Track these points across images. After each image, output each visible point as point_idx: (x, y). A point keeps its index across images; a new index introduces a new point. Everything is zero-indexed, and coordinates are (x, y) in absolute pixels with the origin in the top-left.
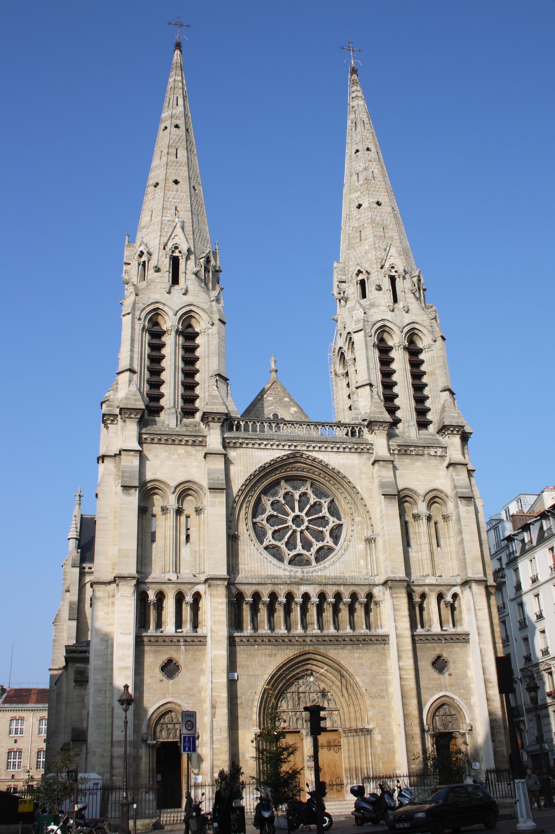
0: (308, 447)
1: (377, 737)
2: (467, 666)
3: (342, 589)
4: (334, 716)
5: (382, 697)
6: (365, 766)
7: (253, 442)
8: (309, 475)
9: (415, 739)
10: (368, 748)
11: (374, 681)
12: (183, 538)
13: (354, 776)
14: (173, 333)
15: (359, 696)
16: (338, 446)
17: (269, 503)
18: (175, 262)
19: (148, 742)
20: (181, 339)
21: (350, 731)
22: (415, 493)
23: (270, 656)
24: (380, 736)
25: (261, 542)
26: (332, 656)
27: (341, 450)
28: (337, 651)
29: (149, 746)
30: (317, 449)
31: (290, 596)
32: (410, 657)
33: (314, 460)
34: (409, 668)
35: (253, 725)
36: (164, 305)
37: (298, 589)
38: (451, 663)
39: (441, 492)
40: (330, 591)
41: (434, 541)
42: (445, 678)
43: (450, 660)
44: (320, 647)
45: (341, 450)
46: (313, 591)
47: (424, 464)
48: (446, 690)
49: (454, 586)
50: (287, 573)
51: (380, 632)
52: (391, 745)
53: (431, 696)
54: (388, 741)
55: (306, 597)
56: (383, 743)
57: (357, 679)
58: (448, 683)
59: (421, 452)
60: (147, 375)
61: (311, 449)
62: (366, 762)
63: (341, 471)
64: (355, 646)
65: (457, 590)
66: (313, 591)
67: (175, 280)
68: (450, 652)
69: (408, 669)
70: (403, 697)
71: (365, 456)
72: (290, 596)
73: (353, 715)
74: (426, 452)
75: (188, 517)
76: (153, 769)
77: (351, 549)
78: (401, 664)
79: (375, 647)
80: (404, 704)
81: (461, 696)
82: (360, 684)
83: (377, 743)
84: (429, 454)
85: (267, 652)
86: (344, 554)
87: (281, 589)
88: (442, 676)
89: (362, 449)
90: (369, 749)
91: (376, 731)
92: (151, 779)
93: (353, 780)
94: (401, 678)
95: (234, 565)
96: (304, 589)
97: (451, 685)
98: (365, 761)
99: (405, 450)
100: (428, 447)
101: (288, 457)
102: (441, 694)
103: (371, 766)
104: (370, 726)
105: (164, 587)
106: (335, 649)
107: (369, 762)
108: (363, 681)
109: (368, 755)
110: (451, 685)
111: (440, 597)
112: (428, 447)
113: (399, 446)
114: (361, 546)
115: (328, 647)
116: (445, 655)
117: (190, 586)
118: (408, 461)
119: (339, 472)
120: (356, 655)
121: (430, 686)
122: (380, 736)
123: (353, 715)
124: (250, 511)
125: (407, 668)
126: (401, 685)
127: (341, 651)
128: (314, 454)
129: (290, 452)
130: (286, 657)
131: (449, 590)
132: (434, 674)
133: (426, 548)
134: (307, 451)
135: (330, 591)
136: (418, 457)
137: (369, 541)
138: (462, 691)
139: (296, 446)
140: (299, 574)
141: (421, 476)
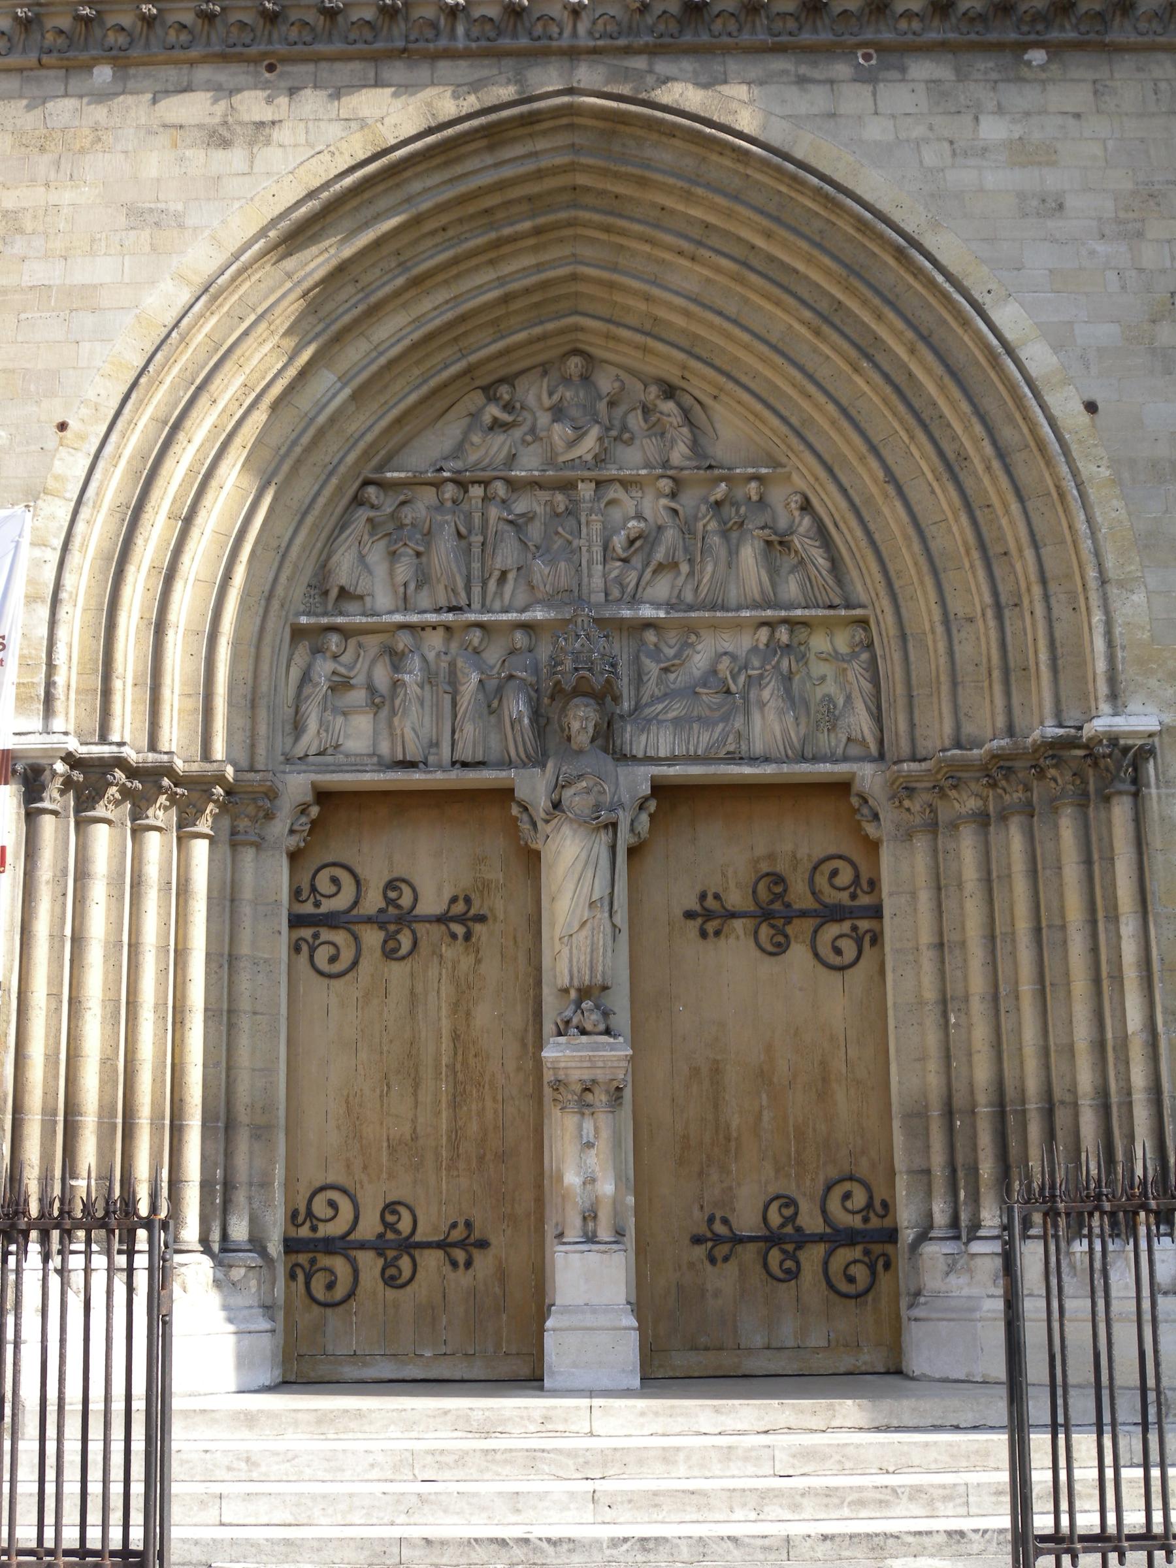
4: (819, 668)
6: (1086, 1080)
10: (1114, 918)
13: (987, 1168)
15: (1029, 471)
23: (219, 138)
28: (816, 99)
57: (1010, 317)
62: (1100, 1046)
64: (983, 64)
82: (1039, 358)
90: (1128, 928)
93: (975, 1198)
98: (1082, 1033)
103: (1139, 1077)
104: (1138, 719)
106: (802, 81)
107: (1124, 1041)
109: (1118, 978)
120: (993, 130)
127: (855, 98)
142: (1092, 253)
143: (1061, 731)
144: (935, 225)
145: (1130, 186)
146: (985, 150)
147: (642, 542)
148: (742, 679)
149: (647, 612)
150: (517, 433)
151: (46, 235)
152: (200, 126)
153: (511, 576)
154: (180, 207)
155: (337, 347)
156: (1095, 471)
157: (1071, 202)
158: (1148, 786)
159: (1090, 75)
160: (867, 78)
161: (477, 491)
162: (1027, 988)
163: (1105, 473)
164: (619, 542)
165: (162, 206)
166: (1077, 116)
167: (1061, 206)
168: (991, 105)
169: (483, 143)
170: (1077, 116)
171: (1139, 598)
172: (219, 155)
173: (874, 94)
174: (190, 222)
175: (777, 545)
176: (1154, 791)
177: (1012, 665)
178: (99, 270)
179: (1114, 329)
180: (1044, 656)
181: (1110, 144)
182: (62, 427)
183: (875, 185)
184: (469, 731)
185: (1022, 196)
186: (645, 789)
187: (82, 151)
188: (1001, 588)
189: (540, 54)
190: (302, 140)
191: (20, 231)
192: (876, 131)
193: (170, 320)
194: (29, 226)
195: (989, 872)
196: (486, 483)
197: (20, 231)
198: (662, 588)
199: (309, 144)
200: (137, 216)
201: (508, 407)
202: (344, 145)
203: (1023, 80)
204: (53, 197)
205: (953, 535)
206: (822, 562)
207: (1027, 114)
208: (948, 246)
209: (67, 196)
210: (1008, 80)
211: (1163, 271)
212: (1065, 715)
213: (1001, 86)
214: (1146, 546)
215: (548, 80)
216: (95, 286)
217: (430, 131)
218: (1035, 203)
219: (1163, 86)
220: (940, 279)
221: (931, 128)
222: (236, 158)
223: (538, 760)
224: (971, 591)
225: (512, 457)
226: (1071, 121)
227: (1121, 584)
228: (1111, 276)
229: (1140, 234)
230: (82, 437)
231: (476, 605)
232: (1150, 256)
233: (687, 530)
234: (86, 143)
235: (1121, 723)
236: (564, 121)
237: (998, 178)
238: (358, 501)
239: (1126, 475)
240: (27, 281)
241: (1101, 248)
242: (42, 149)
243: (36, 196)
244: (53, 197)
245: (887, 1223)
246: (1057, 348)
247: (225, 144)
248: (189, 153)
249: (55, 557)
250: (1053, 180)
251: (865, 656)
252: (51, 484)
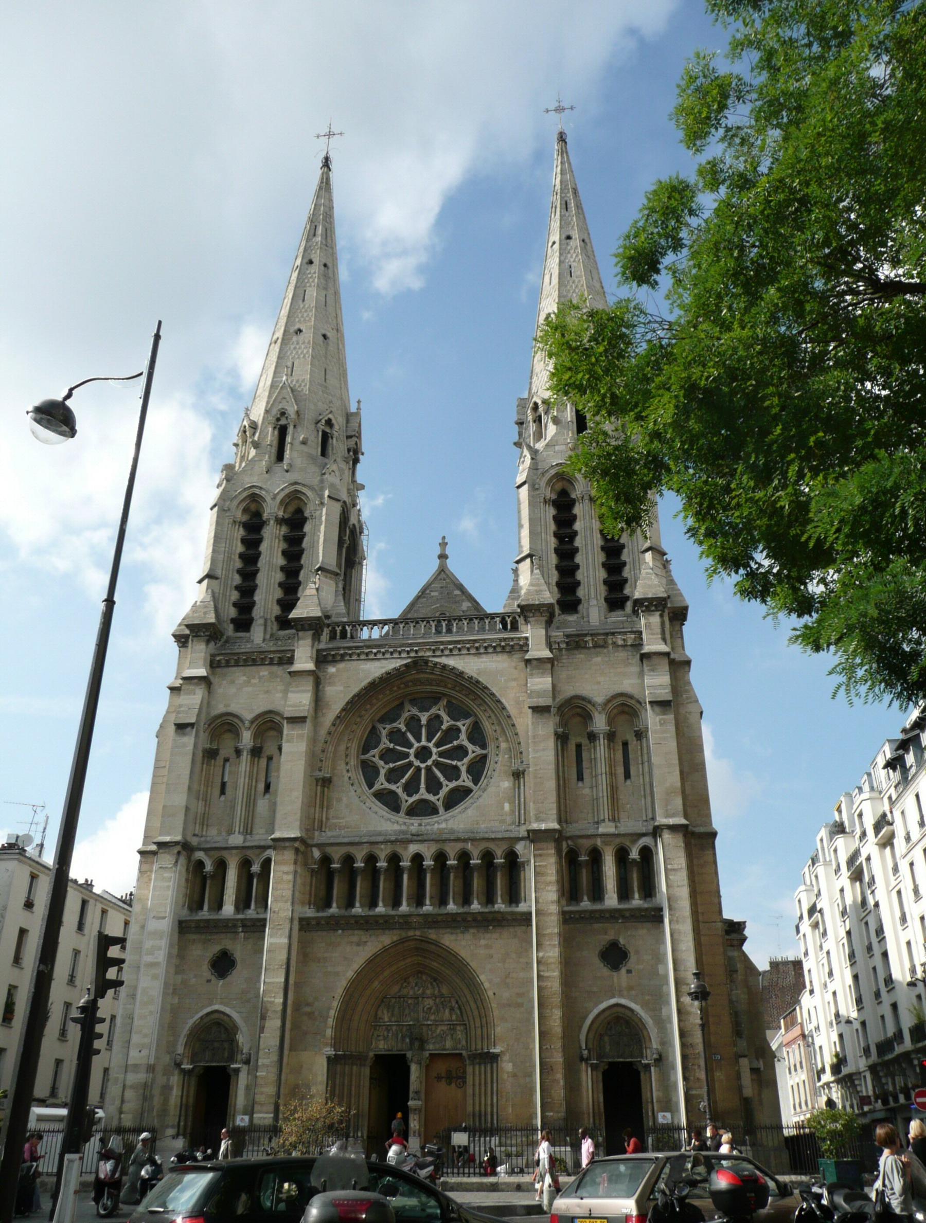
0: (434, 651)
2: (659, 958)
3: (469, 846)
5: (520, 1005)
7: (358, 651)
8: (440, 689)
12: (261, 786)
14: (272, 522)
16: (477, 645)
17: (384, 733)
18: (282, 432)
19: (183, 1067)
20: (284, 530)
22: (590, 702)
25: (370, 788)
26: (447, 943)
27: (482, 650)
28: (453, 937)
29: (183, 1071)
30: (447, 652)
31: (394, 859)
33: (444, 667)
35: (326, 1044)
36: (261, 488)
37: (406, 849)
38: (632, 954)
39: (631, 697)
40: (452, 851)
41: (620, 770)
42: (621, 977)
43: (631, 950)
44: (430, 931)
45: (482, 650)
46: (428, 852)
47: (607, 659)
48: (621, 996)
49: (644, 835)
50: (396, 827)
51: (522, 907)
52: (528, 1079)
53: (596, 1005)
55: (418, 858)
56: (515, 1075)
57: (483, 978)
58: (624, 984)
59: (601, 643)
60: (237, 580)
61: (439, 653)
63: (480, 679)
65: (646, 841)
66: (428, 852)
67: (280, 457)
68: (634, 939)
71: (517, 656)
72: (394, 859)
74: (610, 642)
75: (270, 758)
76: (187, 1106)
77: (491, 789)
79: (511, 930)
81: (644, 1005)
82: (487, 985)
83: (505, 1076)
84: (614, 643)
85: (355, 939)
86: (480, 796)
87: (382, 850)
88: (615, 974)
89: (512, 646)
91: (506, 1057)
92: (183, 1118)
95: (324, 819)
96: (413, 848)
97: (630, 988)
99: (576, 643)
100: (613, 634)
101: (406, 665)
102: (613, 1001)
105: (225, 854)
106: (452, 933)
108: (490, 982)
110: (630, 988)
111: (622, 856)
112: (613, 634)
113: (567, 636)
114: (506, 784)
115: (442, 931)
116: (622, 941)
117: (258, 851)
118: (582, 656)
119: (478, 682)
120: (483, 942)
121: (595, 989)
122: (510, 1064)
124: (354, 747)
127: (460, 936)
128: (444, 660)
129: (409, 660)
130: (380, 946)
131: (634, 842)
132: (605, 971)
133: (603, 781)
134: (434, 656)
135: (452, 851)
136: (598, 650)
137: (518, 775)
138: (647, 997)
139: (416, 652)
140: (414, 829)
141: (600, 679)
160: (463, 933)
183: (464, 953)
189: (410, 929)
192: (464, 943)
215: (411, 933)
238: (382, 1001)
241: (499, 964)
246: (490, 983)
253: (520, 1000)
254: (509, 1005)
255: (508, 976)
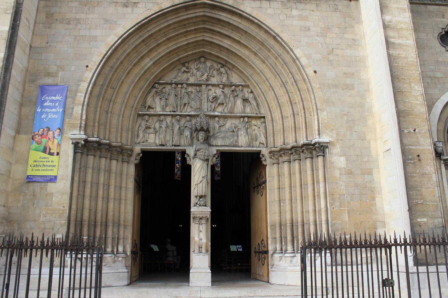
1: (337, 159)
4: (254, 127)
5: (349, 87)
6: (311, 219)
9: (423, 162)
10: (318, 182)
11: (331, 57)
13: (289, 238)
15: (302, 85)
21: (283, 151)
24: (343, 159)
26: (248, 10)
32: (404, 10)
34: (403, 26)
54: (363, 168)
57: (298, 52)
62: (315, 211)
69: (402, 29)
70: (395, 78)
73: (289, 122)
78: (387, 18)
80: (397, 93)
82: (304, 61)
83: (337, 173)
90: (322, 185)
93: (286, 244)
94: (388, 44)
98: (311, 208)
103: (324, 218)
104: (324, 139)
107: (320, 211)
109: (319, 196)
120: (295, 12)
122: (343, 159)
123: (289, 122)
125: (399, 26)
126: (389, 56)
142: (316, 39)
143: (308, 142)
144: (282, 32)
145: (324, 26)
146: (293, 17)
147: (215, 98)
148: (237, 129)
149: (216, 114)
150: (189, 74)
151: (86, 24)
152: (121, 3)
153: (186, 105)
154: (116, 20)
155: (150, 53)
156: (316, 86)
157: (311, 28)
158: (326, 154)
159: (316, 3)
161: (180, 86)
162: (299, 198)
163: (318, 86)
164: (210, 98)
165: (112, 19)
166: (313, 11)
167: (309, 29)
168: (295, 7)
169: (184, 9)
170: (313, 11)
171: (325, 113)
172: (125, 9)
173: (270, 4)
174: (118, 23)
175: (245, 100)
176: (328, 155)
177: (297, 127)
178: (98, 32)
179: (320, 56)
180: (304, 125)
181: (320, 17)
182: (87, 66)
184: (176, 138)
185: (301, 27)
186: (215, 152)
187: (95, 6)
188: (294, 110)
190: (144, 7)
191: (80, 23)
192: (270, 11)
193: (112, 44)
194: (82, 22)
195: (290, 172)
196: (182, 84)
197: (80, 23)
198: (220, 109)
199: (145, 7)
200: (106, 21)
201: (187, 68)
202: (153, 8)
203: (302, 3)
204: (88, 16)
205: (284, 99)
206: (255, 104)
207: (302, 10)
208: (285, 36)
209: (91, 16)
210: (298, 2)
211: (330, 44)
212: (308, 138)
213: (297, 4)
214: (327, 102)
216: (96, 36)
217: (173, 6)
218: (304, 28)
219: (331, 6)
220: (283, 43)
221: (282, 11)
222: (129, 10)
223: (191, 145)
224: (288, 111)
225: (188, 79)
226: (311, 12)
227: (321, 110)
228: (320, 44)
229: (326, 36)
230: (92, 69)
231: (179, 111)
232: (328, 41)
233: (225, 96)
234: (96, 5)
235: (321, 140)
236: (202, 6)
237: (296, 23)
239: (322, 87)
240: (80, 34)
241: (317, 38)
242: (86, 6)
243: (83, 16)
244: (88, 16)
245: (265, 249)
246: (308, 59)
247: (127, 6)
248: (119, 8)
249: (83, 95)
250: (308, 24)
251: (264, 125)
252: (84, 79)
253: (348, 81)
254: (336, 86)
255: (331, 52)
